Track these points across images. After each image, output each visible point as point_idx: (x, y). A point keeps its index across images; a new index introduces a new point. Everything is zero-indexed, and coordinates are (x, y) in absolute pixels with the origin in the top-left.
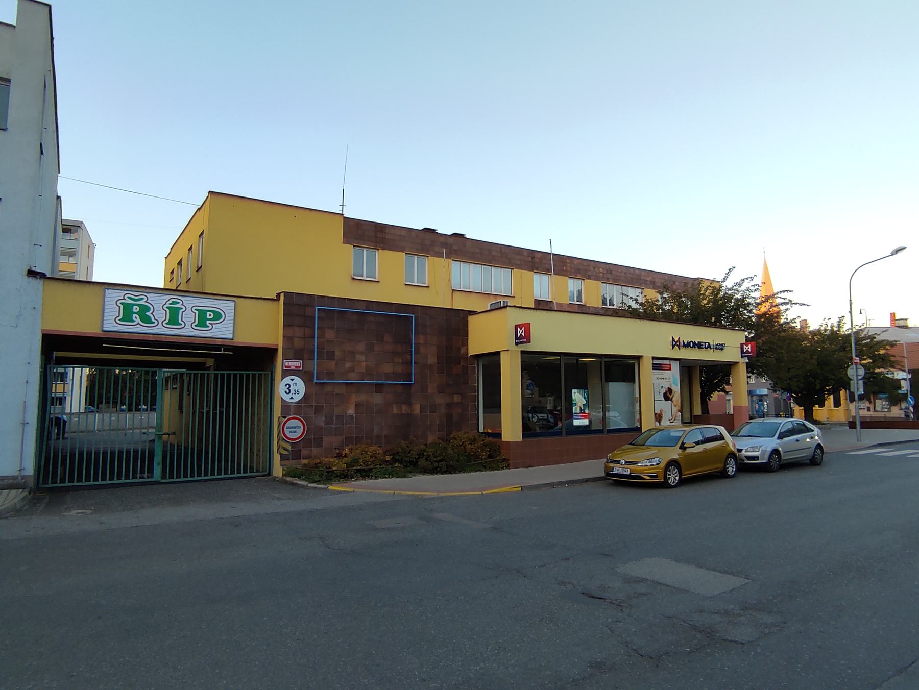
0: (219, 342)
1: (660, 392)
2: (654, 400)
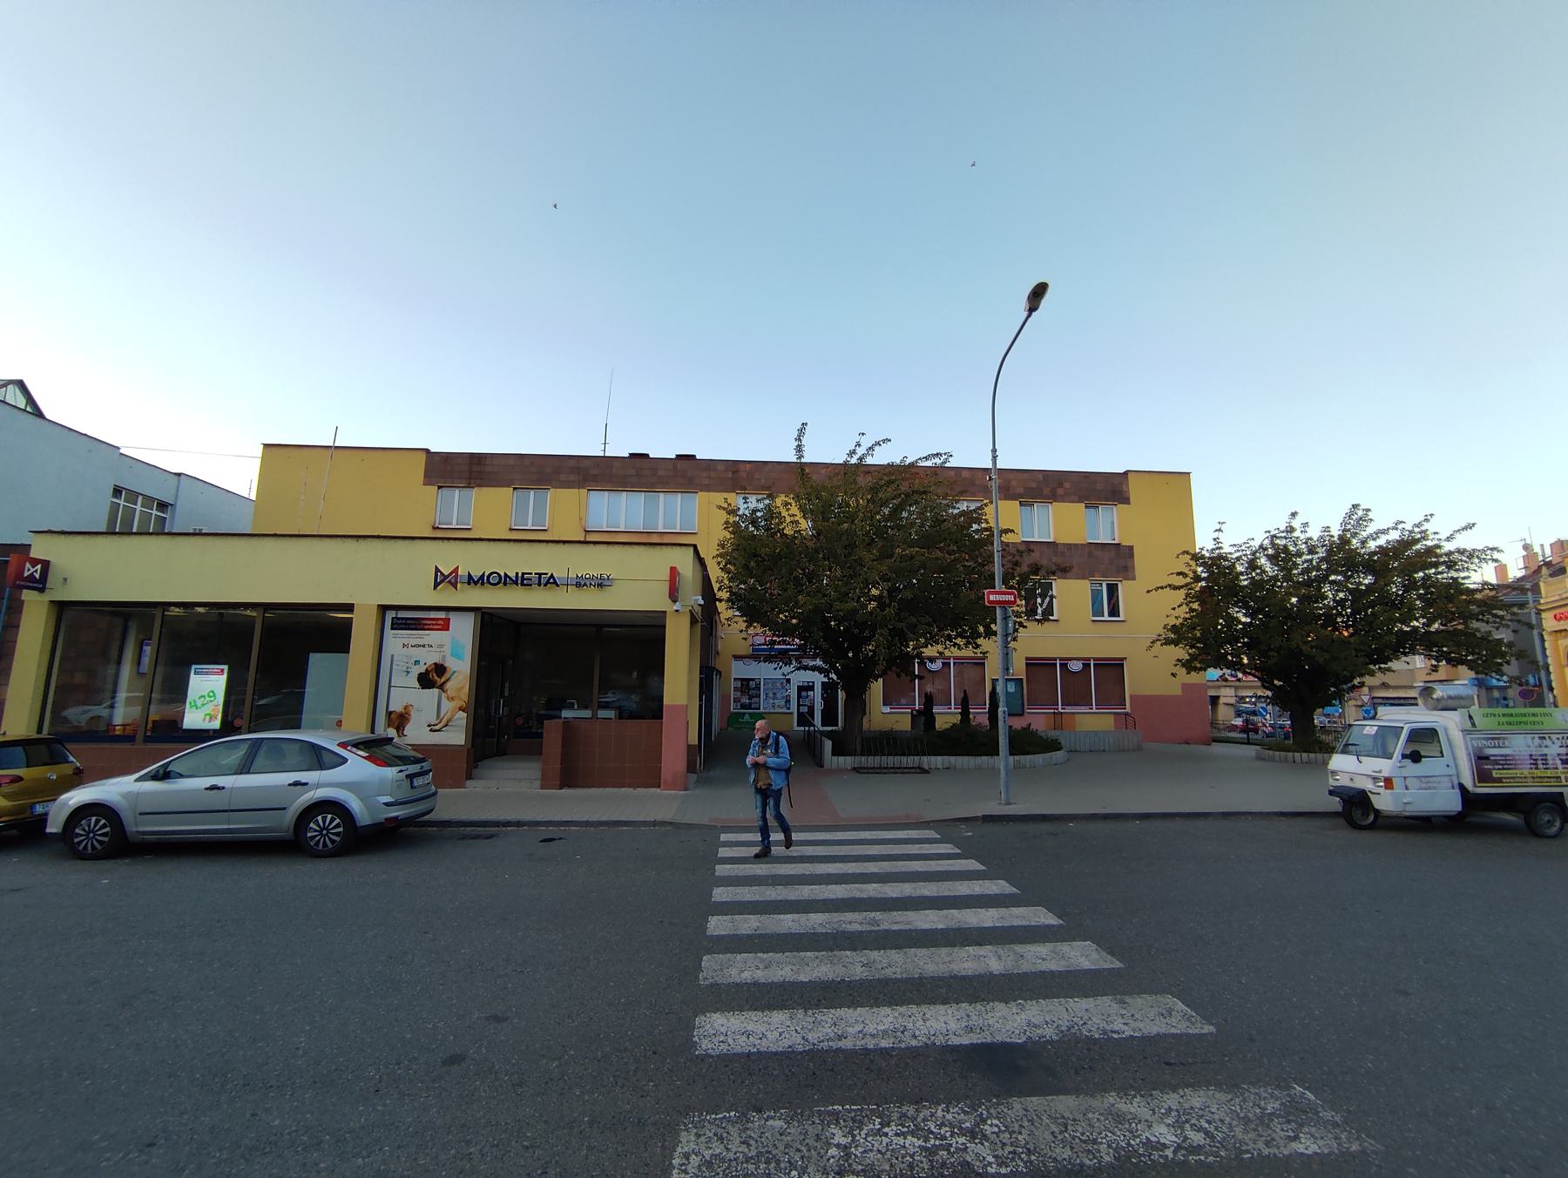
1: (408, 672)
2: (390, 687)
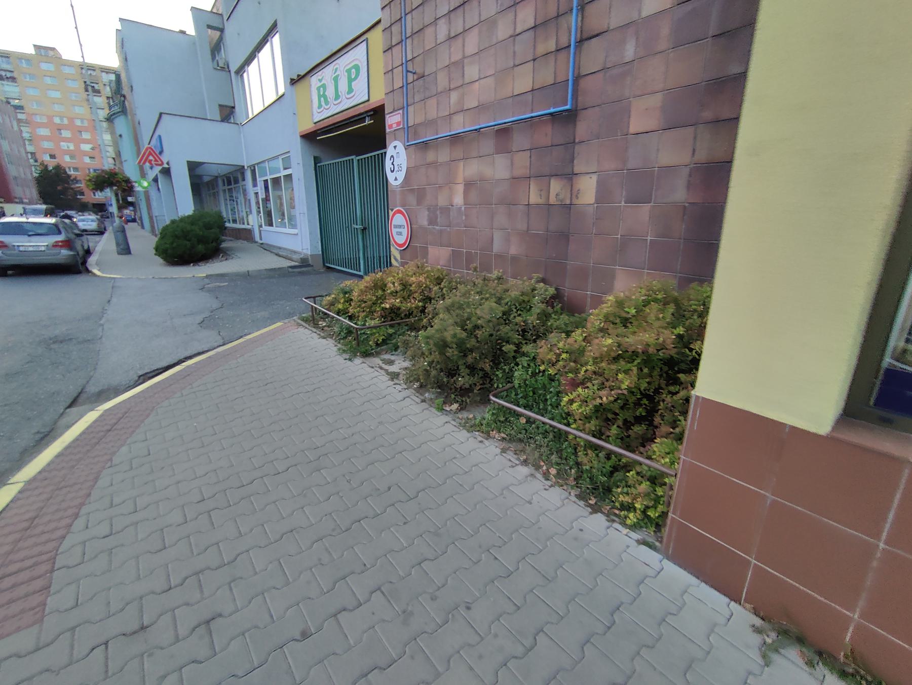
0: (362, 109)
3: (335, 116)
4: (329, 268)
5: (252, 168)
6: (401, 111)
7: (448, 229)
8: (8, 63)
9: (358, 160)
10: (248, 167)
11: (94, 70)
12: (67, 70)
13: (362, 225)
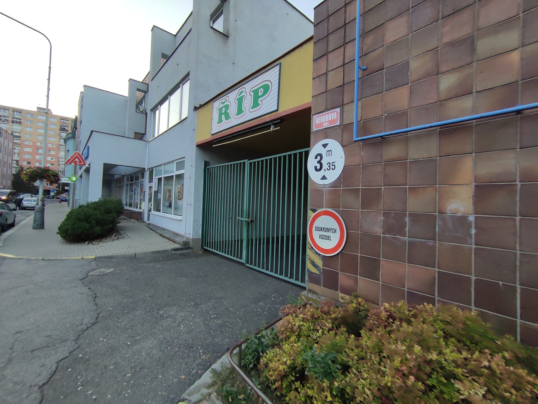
0: (267, 118)
3: (235, 127)
4: (206, 250)
5: (151, 170)
6: (338, 110)
7: (430, 243)
8: (20, 115)
9: (251, 163)
10: (147, 169)
11: (67, 120)
12: (52, 120)
13: (249, 218)
